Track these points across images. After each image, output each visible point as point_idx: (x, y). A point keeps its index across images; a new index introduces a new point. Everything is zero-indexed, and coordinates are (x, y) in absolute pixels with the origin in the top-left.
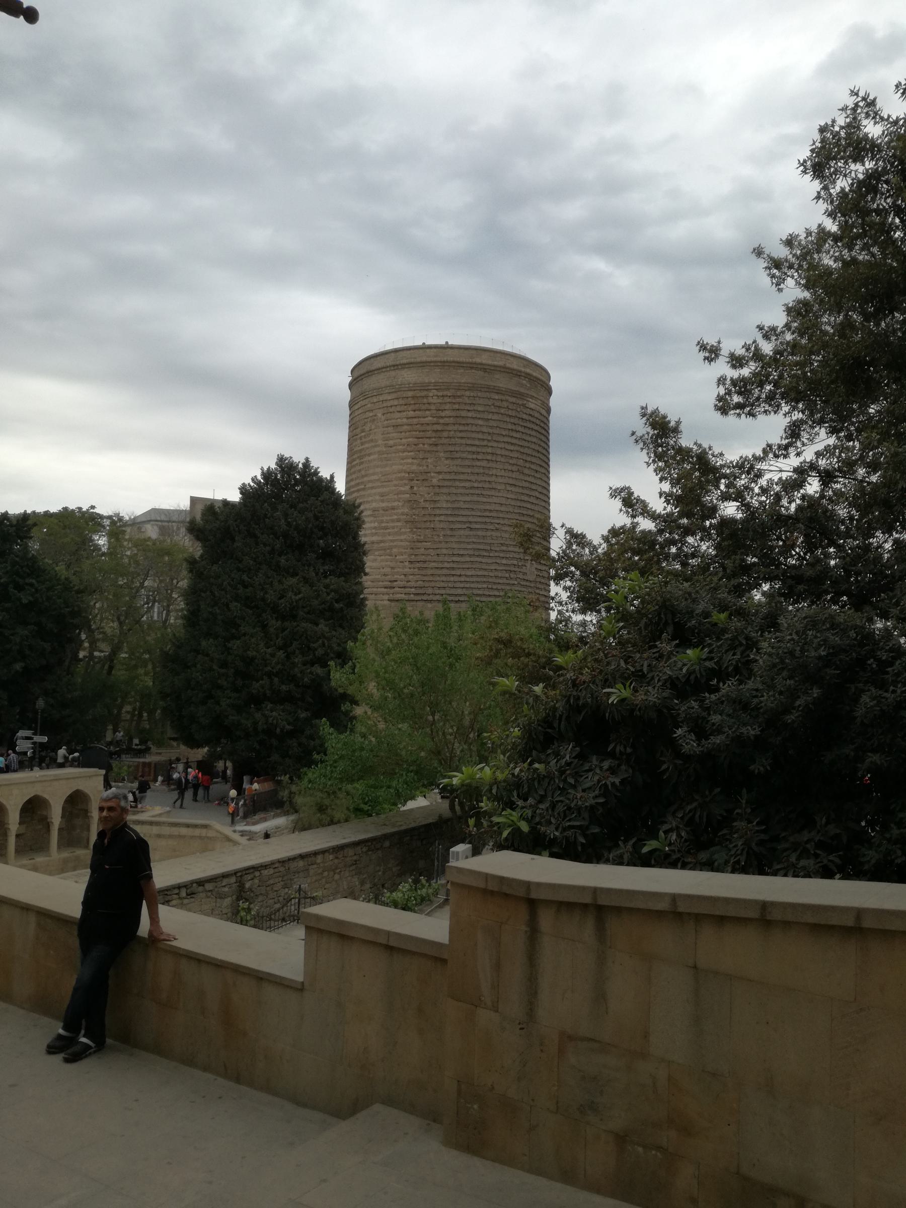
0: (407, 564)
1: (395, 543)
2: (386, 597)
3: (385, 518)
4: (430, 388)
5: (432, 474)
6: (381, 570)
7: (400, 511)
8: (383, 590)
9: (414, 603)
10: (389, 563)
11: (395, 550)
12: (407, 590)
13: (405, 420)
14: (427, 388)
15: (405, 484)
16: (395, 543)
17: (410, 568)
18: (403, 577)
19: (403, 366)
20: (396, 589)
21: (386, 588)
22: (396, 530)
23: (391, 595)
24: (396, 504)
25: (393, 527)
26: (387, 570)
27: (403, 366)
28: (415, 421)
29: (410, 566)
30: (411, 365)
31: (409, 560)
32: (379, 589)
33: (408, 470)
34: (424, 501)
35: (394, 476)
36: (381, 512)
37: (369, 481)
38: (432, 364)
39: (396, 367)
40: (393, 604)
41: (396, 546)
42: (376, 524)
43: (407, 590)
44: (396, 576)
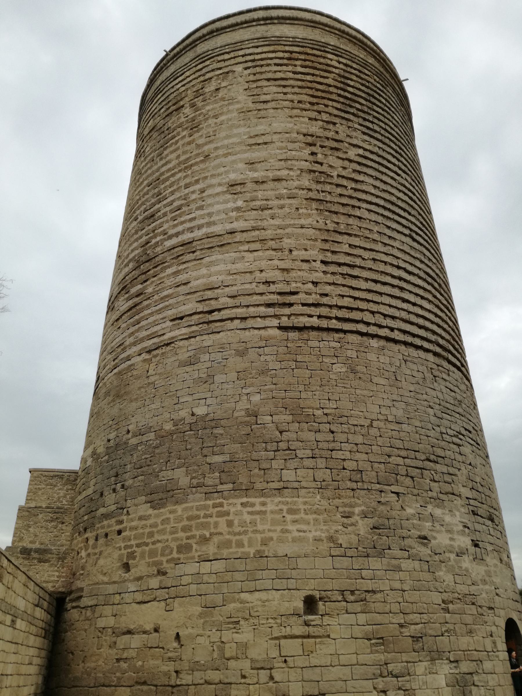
0: (318, 264)
1: (289, 230)
2: (275, 322)
3: (260, 194)
4: (327, 49)
5: (347, 145)
6: (258, 274)
7: (296, 183)
8: (262, 310)
9: (342, 335)
10: (276, 262)
11: (287, 243)
12: (324, 311)
13: (291, 75)
14: (323, 49)
15: (301, 149)
16: (289, 230)
17: (325, 272)
18: (310, 285)
19: (282, 20)
20: (295, 307)
21: (269, 305)
22: (287, 210)
23: (285, 319)
24: (285, 173)
25: (282, 207)
26: (269, 275)
27: (282, 20)
28: (309, 78)
29: (324, 268)
30: (296, 22)
31: (321, 257)
32: (251, 309)
33: (305, 131)
34: (339, 176)
35: (276, 137)
36: (250, 186)
37: (216, 149)
38: (327, 29)
39: (268, 20)
40: (293, 335)
41: (289, 235)
42: (240, 203)
43: (324, 311)
44: (294, 285)
